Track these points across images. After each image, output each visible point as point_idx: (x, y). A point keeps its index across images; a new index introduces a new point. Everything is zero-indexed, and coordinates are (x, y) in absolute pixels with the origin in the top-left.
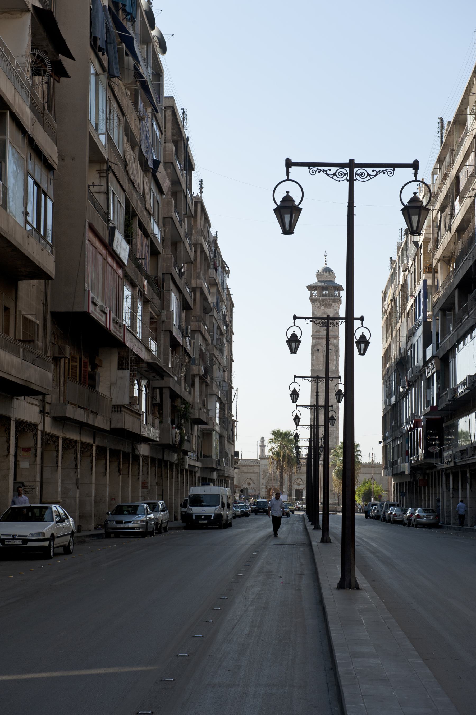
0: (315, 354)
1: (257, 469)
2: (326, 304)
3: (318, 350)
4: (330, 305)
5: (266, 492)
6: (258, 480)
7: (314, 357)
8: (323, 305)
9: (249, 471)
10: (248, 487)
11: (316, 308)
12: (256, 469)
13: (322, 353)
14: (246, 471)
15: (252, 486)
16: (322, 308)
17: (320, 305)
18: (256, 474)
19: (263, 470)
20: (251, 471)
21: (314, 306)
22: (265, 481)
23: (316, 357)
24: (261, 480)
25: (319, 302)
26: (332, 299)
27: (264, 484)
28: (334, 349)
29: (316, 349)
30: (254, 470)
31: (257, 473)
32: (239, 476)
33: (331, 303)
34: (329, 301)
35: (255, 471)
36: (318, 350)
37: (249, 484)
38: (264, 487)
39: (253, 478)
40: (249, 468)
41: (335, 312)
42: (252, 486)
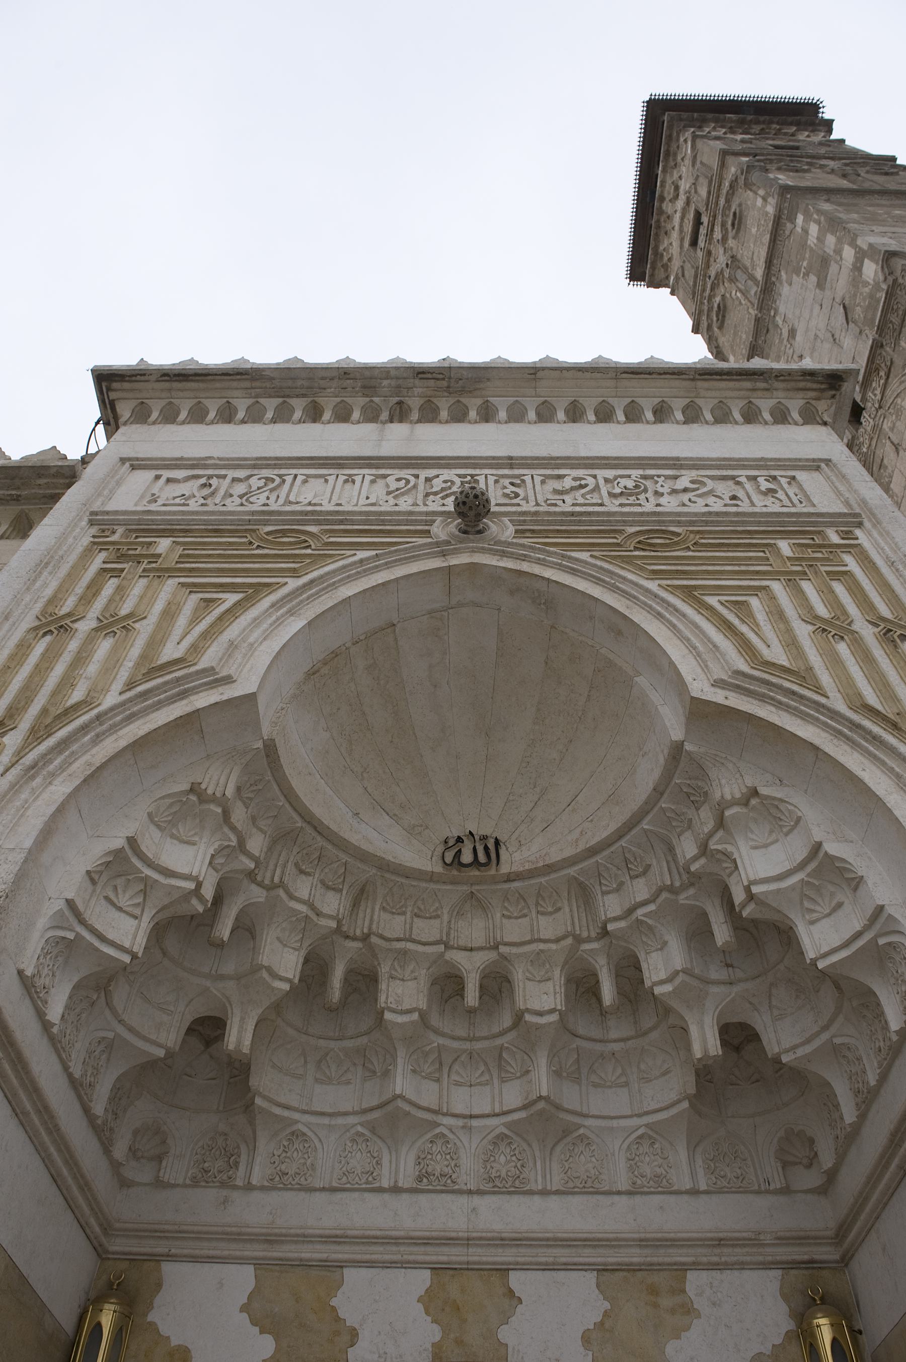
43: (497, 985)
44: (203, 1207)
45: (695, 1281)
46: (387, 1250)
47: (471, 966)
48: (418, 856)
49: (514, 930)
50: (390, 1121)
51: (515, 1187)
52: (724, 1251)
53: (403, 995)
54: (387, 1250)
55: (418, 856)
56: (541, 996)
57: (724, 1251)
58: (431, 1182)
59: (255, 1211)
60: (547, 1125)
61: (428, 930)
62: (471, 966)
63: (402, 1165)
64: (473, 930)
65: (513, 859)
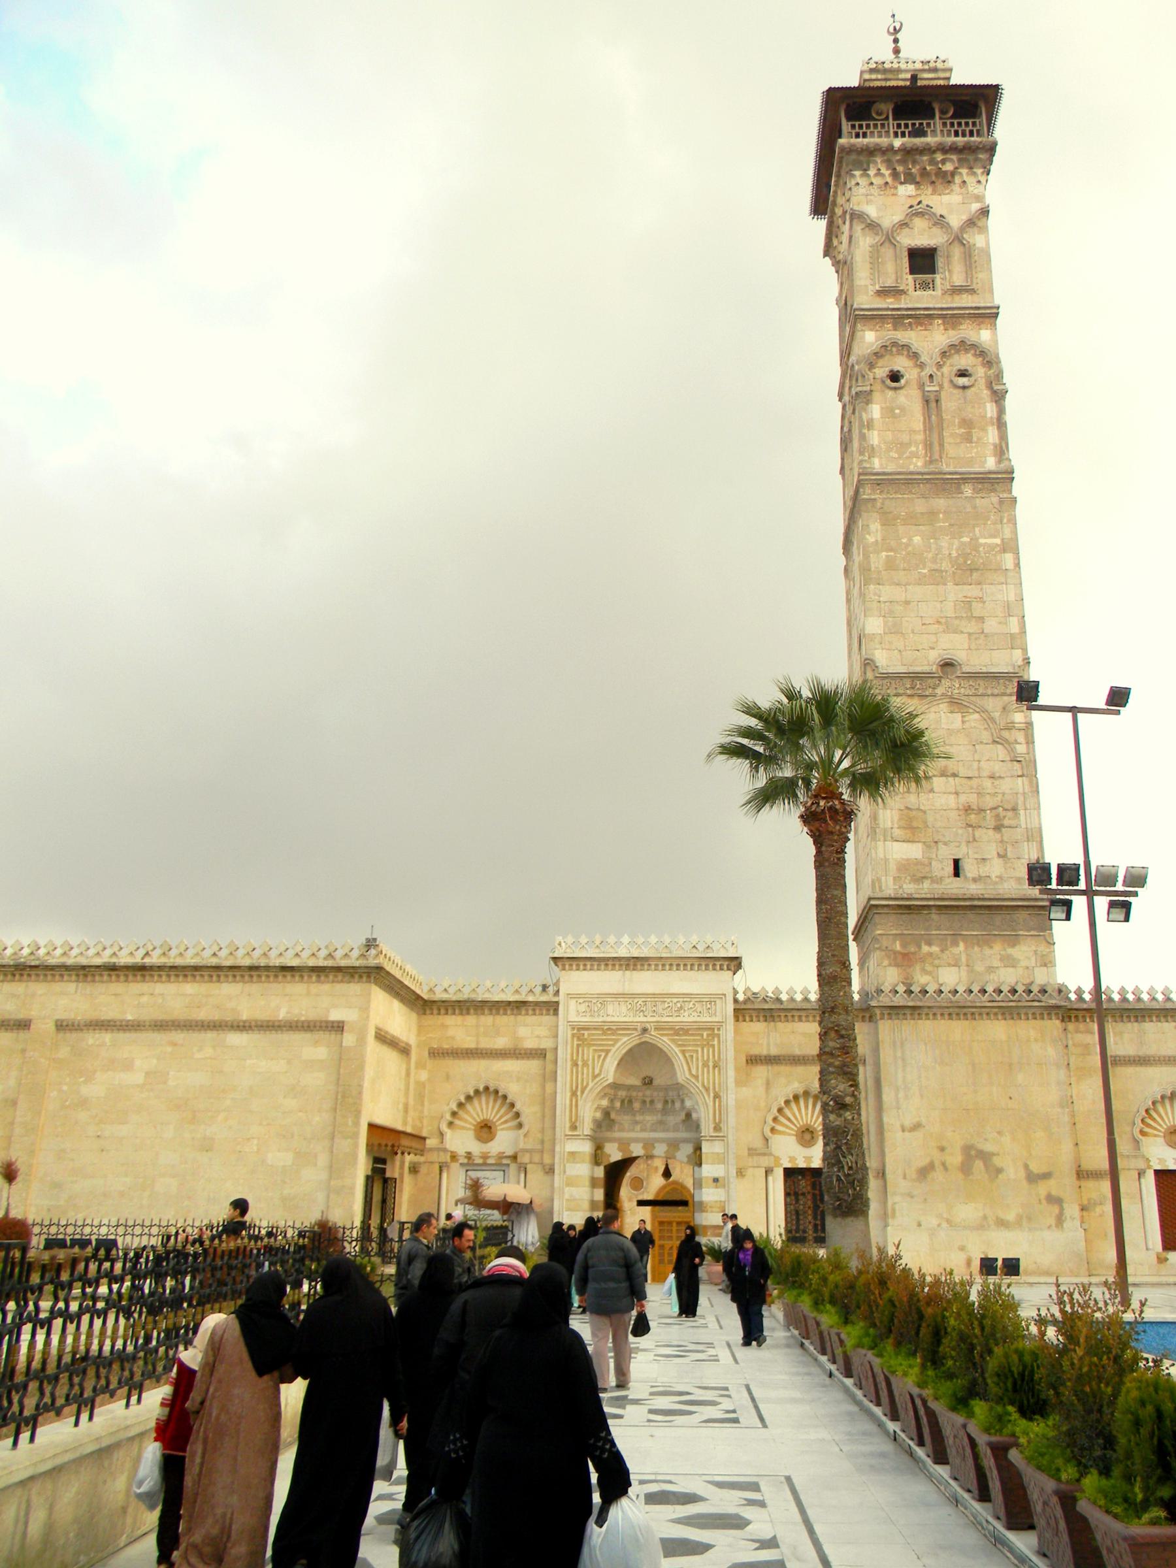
0: (876, 396)
1: (543, 1031)
2: (924, 173)
3: (895, 377)
4: (947, 179)
5: (594, 1183)
6: (548, 1104)
7: (875, 411)
8: (910, 179)
9: (486, 1043)
10: (476, 1148)
11: (874, 191)
12: (530, 1031)
13: (915, 393)
14: (469, 1043)
15: (503, 1142)
16: (910, 189)
17: (895, 175)
18: (533, 1065)
19: (580, 1032)
20: (501, 1043)
21: (863, 182)
22: (589, 1113)
23: (889, 412)
24: (563, 1099)
25: (889, 164)
26: (953, 149)
27: (587, 1128)
28: (980, 372)
29: (881, 372)
30: (523, 1032)
31: (540, 1054)
32: (424, 1076)
33: (949, 167)
34: (939, 157)
35: (530, 1044)
36: (895, 377)
37: (486, 1130)
38: (586, 1148)
39: (512, 1089)
40: (487, 1020)
41: (975, 206)
42: (503, 1142)
43: (652, 1102)
44: (609, 1134)
45: (681, 1145)
46: (636, 1140)
47: (648, 1100)
48: (636, 1082)
49: (655, 1094)
50: (637, 1123)
51: (654, 1131)
52: (685, 1141)
53: (637, 1105)
54: (636, 1140)
55: (636, 1082)
56: (659, 1106)
57: (685, 1141)
58: (642, 1130)
59: (617, 1135)
60: (661, 1122)
61: (640, 1094)
62: (648, 1100)
63: (638, 1127)
64: (648, 1093)
65: (655, 1083)
